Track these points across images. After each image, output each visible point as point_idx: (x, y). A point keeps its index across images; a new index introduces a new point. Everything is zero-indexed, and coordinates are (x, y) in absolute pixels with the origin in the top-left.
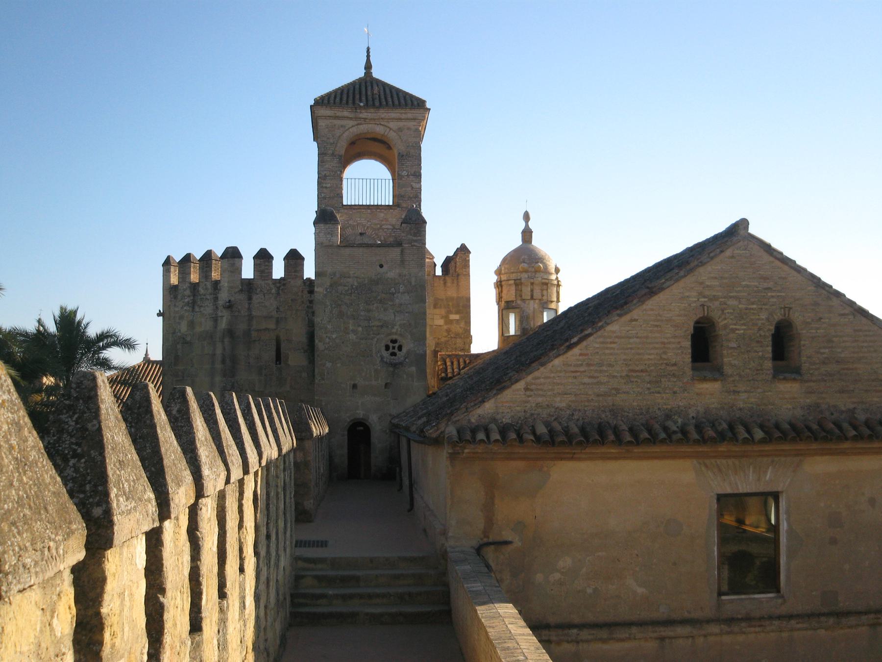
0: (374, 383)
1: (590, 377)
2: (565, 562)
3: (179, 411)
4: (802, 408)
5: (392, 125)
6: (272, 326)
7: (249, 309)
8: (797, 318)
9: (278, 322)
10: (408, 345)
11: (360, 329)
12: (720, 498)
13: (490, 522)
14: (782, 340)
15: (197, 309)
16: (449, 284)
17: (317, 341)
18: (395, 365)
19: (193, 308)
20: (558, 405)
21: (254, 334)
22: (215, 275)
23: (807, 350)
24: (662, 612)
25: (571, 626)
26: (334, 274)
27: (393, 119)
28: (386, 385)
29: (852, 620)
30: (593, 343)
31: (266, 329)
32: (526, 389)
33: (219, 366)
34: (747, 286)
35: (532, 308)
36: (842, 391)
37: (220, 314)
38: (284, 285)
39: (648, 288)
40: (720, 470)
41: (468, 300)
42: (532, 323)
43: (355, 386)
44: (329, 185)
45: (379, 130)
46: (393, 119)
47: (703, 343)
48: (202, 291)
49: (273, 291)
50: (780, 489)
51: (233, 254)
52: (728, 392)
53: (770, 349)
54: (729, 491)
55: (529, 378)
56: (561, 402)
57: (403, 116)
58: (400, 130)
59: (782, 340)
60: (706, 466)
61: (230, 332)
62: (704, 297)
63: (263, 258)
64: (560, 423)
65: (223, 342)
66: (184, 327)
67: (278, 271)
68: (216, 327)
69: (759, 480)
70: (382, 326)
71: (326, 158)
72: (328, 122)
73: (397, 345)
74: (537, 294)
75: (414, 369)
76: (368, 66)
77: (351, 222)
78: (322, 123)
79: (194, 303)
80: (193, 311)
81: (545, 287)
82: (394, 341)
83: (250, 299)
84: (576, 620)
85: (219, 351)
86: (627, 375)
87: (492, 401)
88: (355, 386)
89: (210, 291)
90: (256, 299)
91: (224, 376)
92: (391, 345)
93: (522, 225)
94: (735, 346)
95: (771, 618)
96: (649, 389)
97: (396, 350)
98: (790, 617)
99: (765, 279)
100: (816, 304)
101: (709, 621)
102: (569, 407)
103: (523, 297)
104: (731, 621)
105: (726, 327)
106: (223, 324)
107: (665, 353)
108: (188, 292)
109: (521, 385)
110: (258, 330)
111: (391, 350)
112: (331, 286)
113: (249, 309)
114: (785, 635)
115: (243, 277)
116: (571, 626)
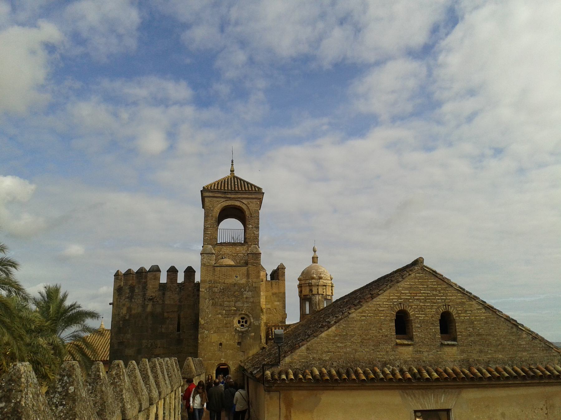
0: (232, 342)
1: (342, 343)
3: (116, 374)
4: (459, 361)
5: (244, 201)
11: (224, 312)
12: (415, 412)
14: (446, 324)
15: (133, 301)
16: (274, 285)
17: (200, 319)
18: (242, 332)
19: (131, 300)
20: (324, 358)
21: (166, 314)
27: (244, 198)
28: (239, 343)
30: (343, 324)
32: (308, 349)
34: (424, 293)
35: (317, 299)
37: (146, 303)
38: (183, 286)
39: (371, 294)
40: (415, 396)
41: (284, 293)
42: (318, 307)
43: (221, 344)
44: (209, 233)
45: (237, 203)
46: (244, 198)
47: (403, 324)
48: (137, 291)
50: (450, 408)
51: (156, 270)
52: (417, 351)
53: (439, 327)
54: (421, 408)
55: (309, 344)
56: (326, 357)
57: (250, 196)
59: (446, 324)
60: (407, 394)
62: (401, 299)
63: (173, 271)
64: (326, 369)
66: (124, 311)
67: (181, 278)
69: (437, 402)
70: (236, 310)
71: (209, 218)
72: (210, 199)
73: (244, 320)
75: (253, 334)
77: (221, 252)
78: (206, 200)
80: (131, 301)
81: (325, 287)
82: (243, 318)
83: (164, 294)
86: (361, 342)
87: (290, 356)
88: (221, 344)
90: (168, 294)
92: (241, 320)
93: (312, 254)
94: (419, 326)
96: (373, 350)
97: (244, 324)
100: (463, 303)
102: (330, 359)
103: (313, 293)
105: (414, 315)
106: (149, 309)
107: (381, 329)
108: (128, 291)
109: (303, 348)
110: (168, 312)
111: (241, 323)
112: (209, 287)
113: (163, 301)
115: (161, 282)
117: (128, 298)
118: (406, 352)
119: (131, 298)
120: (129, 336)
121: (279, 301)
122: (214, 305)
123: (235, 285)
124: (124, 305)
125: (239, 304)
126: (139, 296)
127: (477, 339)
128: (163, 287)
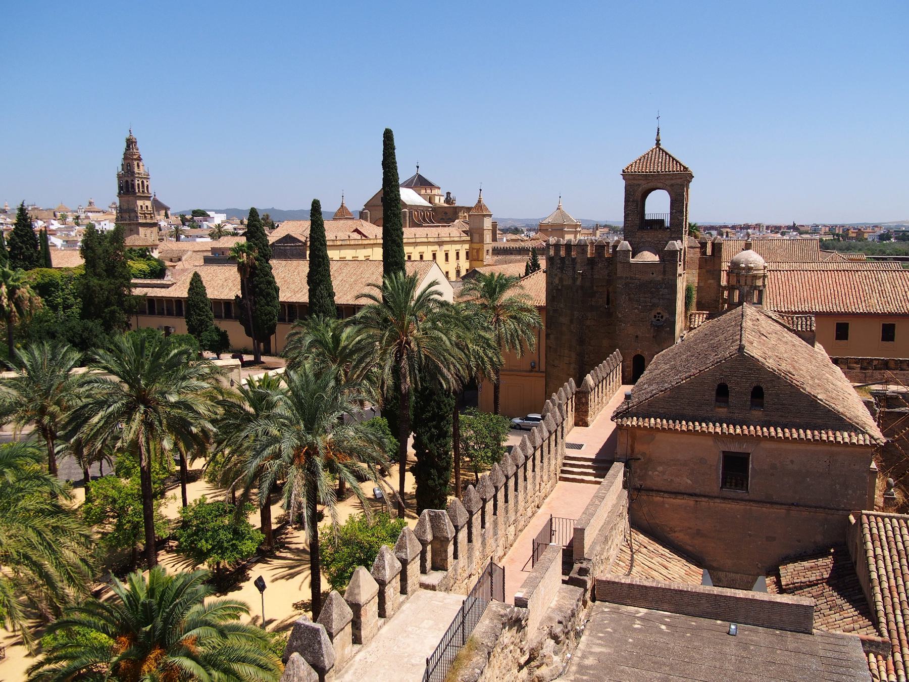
2: (660, 469)
8: (763, 386)
10: (666, 316)
13: (633, 451)
14: (757, 394)
18: (658, 327)
22: (573, 254)
23: (767, 398)
24: (697, 491)
25: (661, 491)
26: (627, 278)
29: (779, 507)
36: (781, 416)
58: (672, 185)
59: (757, 394)
66: (557, 281)
74: (749, 282)
76: (658, 141)
82: (659, 313)
83: (592, 268)
84: (663, 489)
88: (637, 337)
95: (743, 500)
98: (752, 501)
99: (750, 369)
101: (715, 497)
104: (724, 498)
106: (578, 282)
108: (559, 261)
114: (748, 507)
116: (661, 491)
118: (722, 411)
119: (562, 269)
120: (562, 306)
121: (713, 279)
122: (630, 299)
123: (651, 282)
124: (556, 275)
125: (655, 301)
127: (780, 407)
128: (591, 262)
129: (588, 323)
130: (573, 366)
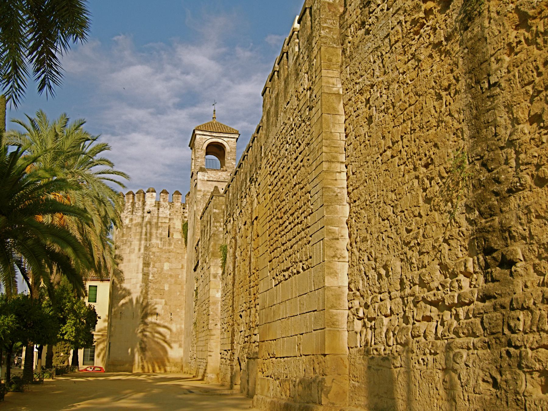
5: (225, 139)
6: (167, 221)
7: (158, 214)
9: (170, 219)
15: (134, 213)
21: (160, 224)
31: (165, 222)
33: (143, 237)
45: (220, 141)
49: (168, 207)
58: (228, 141)
61: (150, 223)
65: (146, 227)
68: (143, 220)
79: (133, 211)
83: (158, 209)
85: (144, 230)
89: (141, 206)
90: (161, 210)
91: (146, 240)
106: (146, 219)
108: (130, 207)
110: (161, 223)
113: (158, 214)
117: (130, 211)
126: (139, 211)
129: (154, 250)
130: (138, 285)
